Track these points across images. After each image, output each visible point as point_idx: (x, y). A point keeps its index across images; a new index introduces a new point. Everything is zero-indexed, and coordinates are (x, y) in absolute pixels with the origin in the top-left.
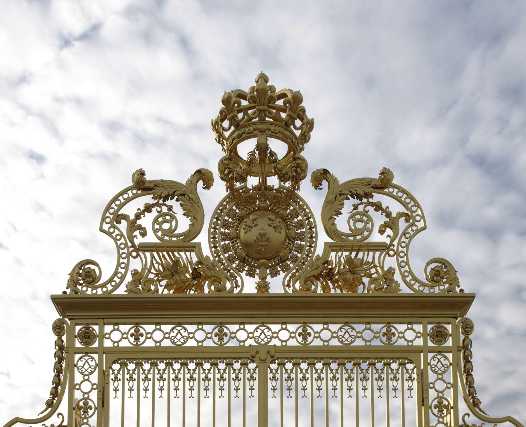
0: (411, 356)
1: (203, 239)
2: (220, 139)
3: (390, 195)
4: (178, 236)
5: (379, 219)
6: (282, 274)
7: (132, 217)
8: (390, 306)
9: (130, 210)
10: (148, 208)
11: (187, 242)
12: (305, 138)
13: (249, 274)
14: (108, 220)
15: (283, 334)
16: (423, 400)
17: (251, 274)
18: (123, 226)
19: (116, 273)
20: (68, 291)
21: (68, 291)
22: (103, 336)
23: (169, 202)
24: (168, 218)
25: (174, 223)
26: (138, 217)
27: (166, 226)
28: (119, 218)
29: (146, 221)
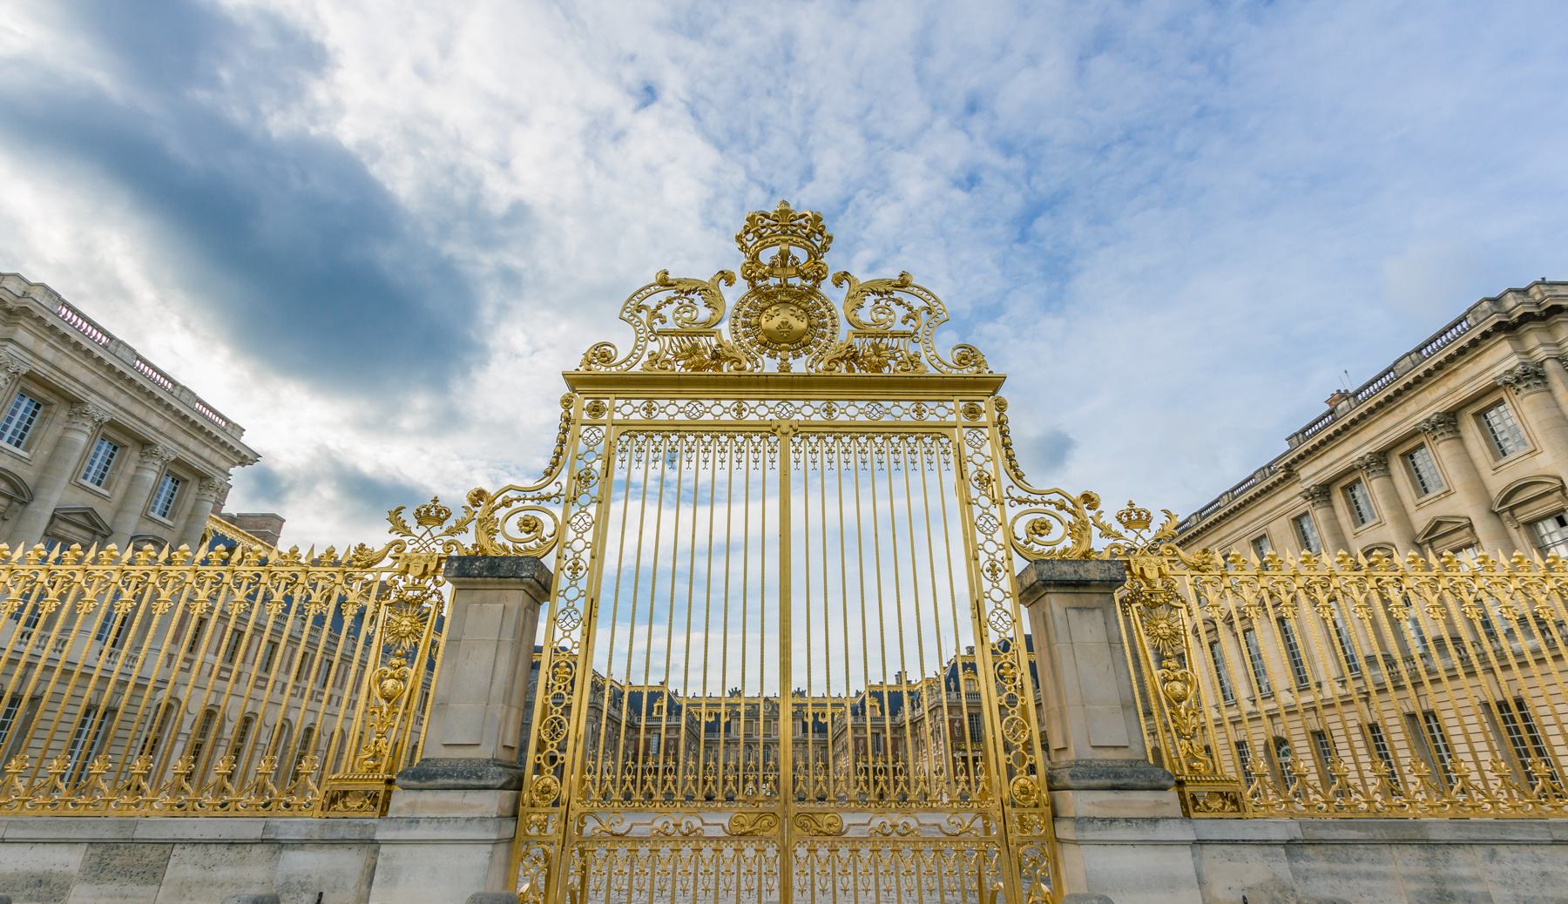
0: (944, 431)
1: (725, 328)
2: (744, 248)
5: (901, 312)
6: (805, 357)
7: (653, 308)
8: (918, 385)
9: (651, 303)
10: (669, 301)
11: (708, 329)
12: (825, 248)
13: (770, 356)
15: (809, 411)
18: (644, 315)
23: (691, 296)
26: (659, 308)
28: (640, 309)
29: (667, 311)
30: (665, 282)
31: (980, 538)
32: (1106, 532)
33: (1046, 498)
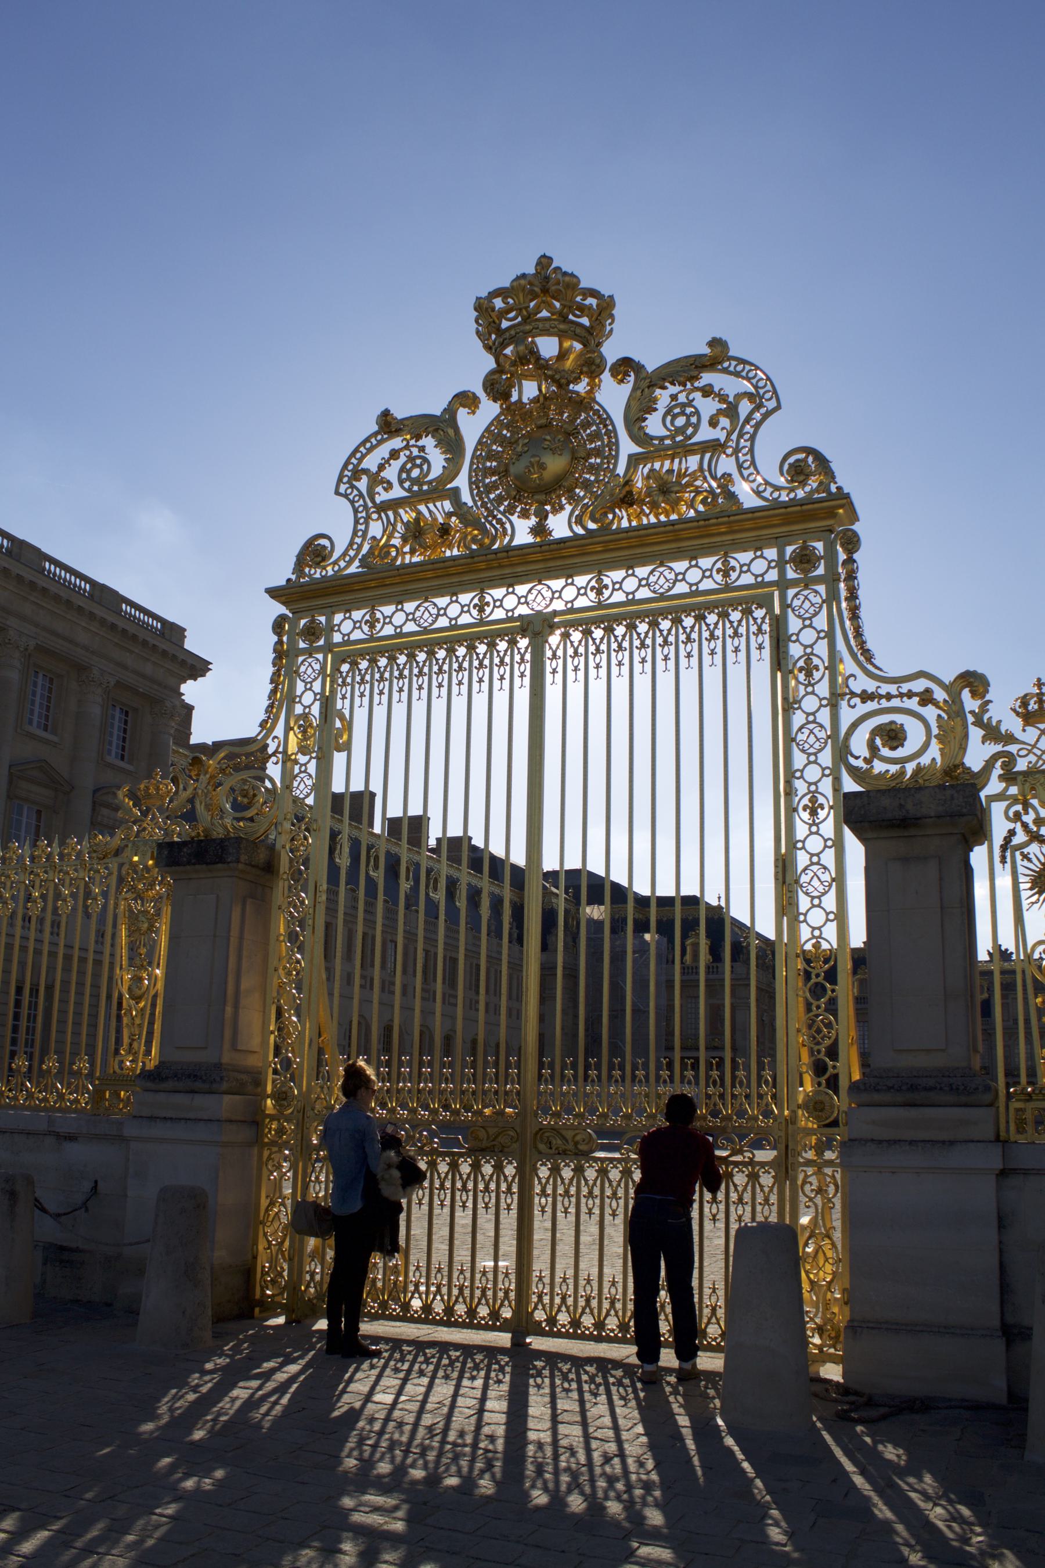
3: (726, 371)
4: (430, 482)
5: (708, 407)
6: (568, 508)
7: (374, 469)
8: (724, 527)
10: (394, 454)
14: (345, 480)
16: (779, 660)
17: (524, 515)
18: (363, 484)
19: (351, 544)
20: (293, 577)
21: (293, 577)
22: (331, 628)
24: (418, 462)
25: (425, 467)
26: (381, 467)
27: (416, 473)
28: (357, 474)
30: (388, 425)
31: (799, 760)
32: (993, 733)
33: (905, 688)
